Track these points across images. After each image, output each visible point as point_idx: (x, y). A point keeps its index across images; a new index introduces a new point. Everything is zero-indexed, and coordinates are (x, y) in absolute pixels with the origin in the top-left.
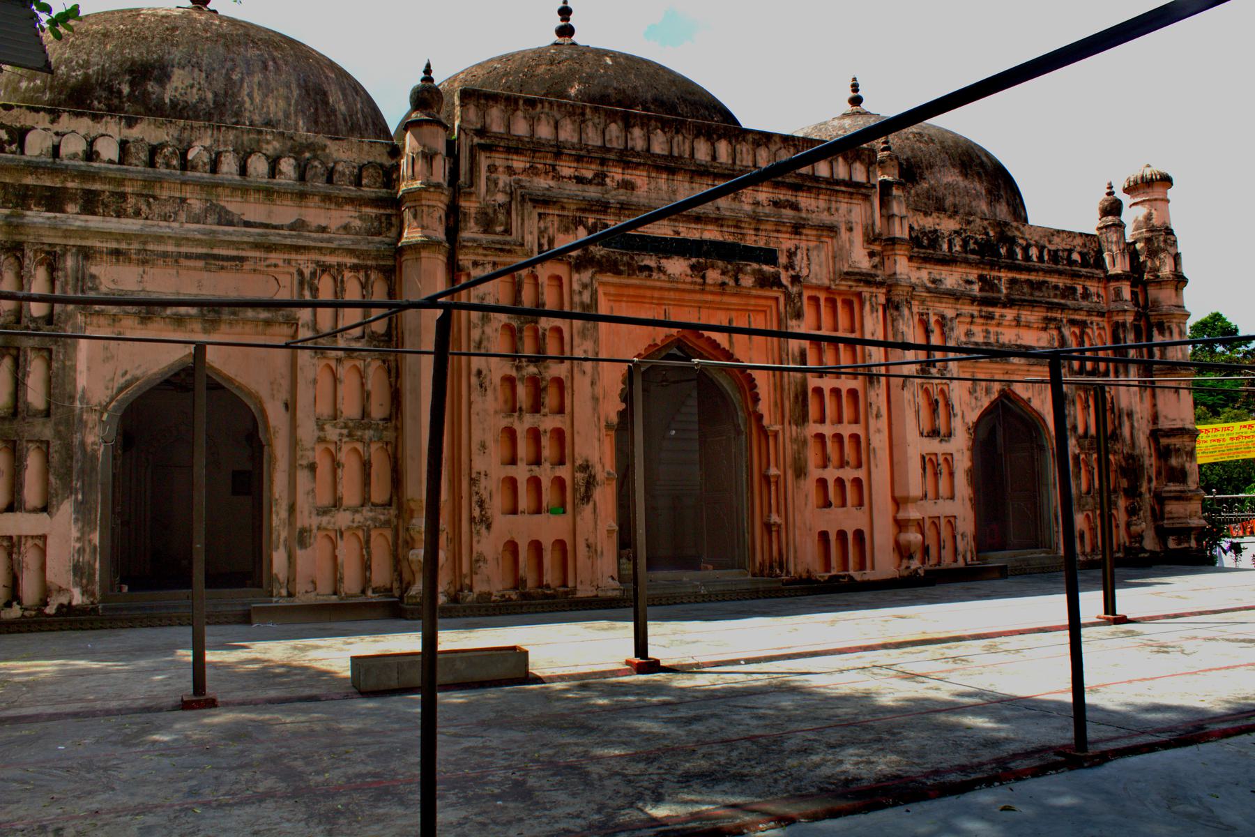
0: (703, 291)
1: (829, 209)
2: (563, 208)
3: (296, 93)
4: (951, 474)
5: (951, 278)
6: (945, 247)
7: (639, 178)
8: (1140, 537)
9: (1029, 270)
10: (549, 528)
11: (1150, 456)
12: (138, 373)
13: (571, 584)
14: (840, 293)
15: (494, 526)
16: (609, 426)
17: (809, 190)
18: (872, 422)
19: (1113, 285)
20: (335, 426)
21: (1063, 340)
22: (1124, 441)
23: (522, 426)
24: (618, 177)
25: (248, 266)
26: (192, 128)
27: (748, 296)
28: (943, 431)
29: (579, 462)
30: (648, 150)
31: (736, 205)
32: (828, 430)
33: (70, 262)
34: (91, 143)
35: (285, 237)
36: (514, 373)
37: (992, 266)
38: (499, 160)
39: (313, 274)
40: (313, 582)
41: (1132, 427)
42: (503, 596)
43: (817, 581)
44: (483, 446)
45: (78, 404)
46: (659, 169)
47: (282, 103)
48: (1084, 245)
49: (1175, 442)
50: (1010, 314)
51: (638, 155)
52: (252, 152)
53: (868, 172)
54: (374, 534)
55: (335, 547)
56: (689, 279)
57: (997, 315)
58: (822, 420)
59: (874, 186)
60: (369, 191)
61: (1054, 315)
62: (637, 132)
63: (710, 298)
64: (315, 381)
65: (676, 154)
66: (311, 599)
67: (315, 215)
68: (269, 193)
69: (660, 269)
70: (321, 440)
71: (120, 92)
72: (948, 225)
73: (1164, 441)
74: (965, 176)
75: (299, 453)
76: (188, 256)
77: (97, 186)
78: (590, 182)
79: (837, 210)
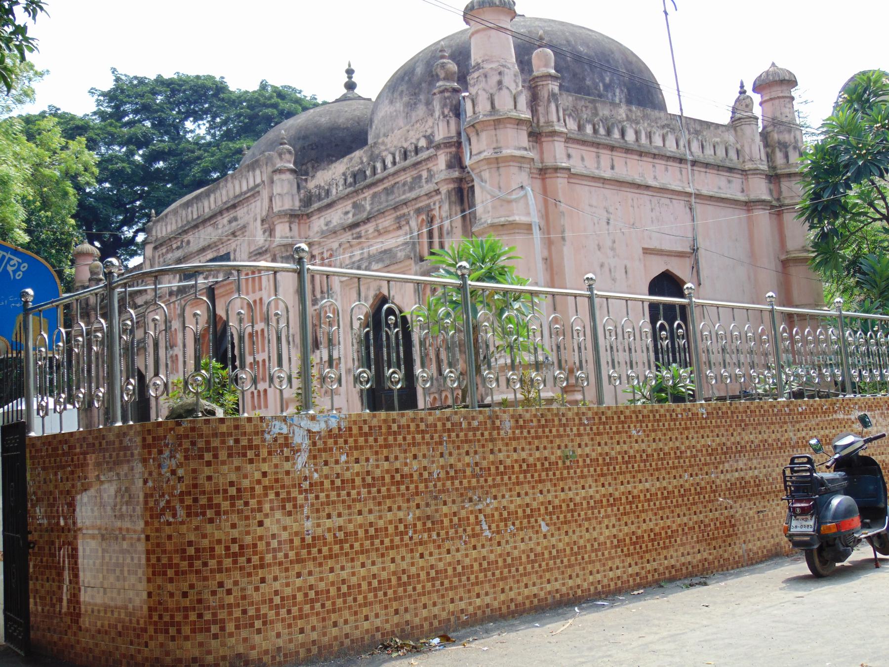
5: (336, 216)
7: (190, 237)
50: (370, 227)
61: (402, 212)
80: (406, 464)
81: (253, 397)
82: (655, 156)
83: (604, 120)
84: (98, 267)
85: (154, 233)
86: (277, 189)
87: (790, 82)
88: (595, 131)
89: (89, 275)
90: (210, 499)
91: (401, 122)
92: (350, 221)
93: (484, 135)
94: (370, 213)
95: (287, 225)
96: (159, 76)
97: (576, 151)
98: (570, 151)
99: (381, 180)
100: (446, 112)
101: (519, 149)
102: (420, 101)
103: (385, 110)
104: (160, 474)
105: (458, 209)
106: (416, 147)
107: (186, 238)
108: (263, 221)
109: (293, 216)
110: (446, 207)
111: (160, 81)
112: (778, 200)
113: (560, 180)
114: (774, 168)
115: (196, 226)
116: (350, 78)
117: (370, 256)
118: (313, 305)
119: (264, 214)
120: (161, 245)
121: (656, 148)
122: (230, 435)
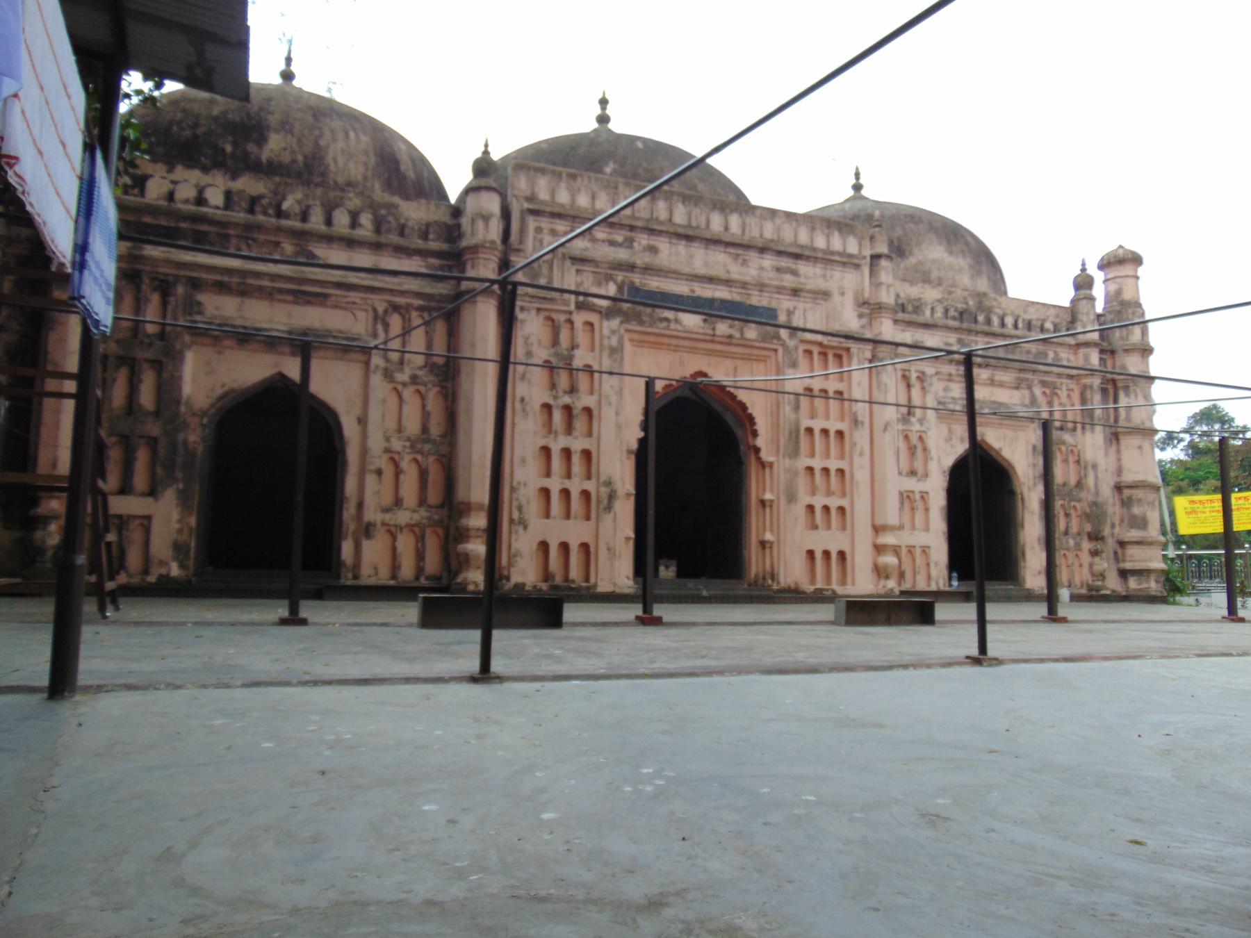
0: (712, 341)
1: (824, 276)
2: (597, 266)
3: (373, 160)
4: (927, 510)
5: (932, 339)
6: (928, 313)
7: (663, 244)
8: (1102, 576)
9: (1004, 336)
10: (575, 532)
11: (1114, 505)
12: (235, 385)
13: (592, 580)
14: (832, 348)
15: (531, 528)
16: (629, 452)
17: (808, 258)
18: (856, 459)
19: (1082, 351)
20: (399, 439)
21: (1034, 401)
22: (1089, 491)
23: (556, 447)
24: (644, 242)
25: (330, 302)
26: (286, 184)
27: (752, 347)
28: (920, 471)
29: (603, 478)
30: (670, 220)
31: (742, 269)
32: (817, 464)
33: (180, 290)
34: (201, 191)
35: (362, 279)
36: (551, 402)
37: (970, 331)
38: (545, 223)
39: (386, 312)
40: (376, 569)
41: (1096, 478)
42: (535, 587)
43: (804, 593)
44: (523, 461)
45: (183, 409)
46: (678, 236)
47: (361, 169)
48: (1058, 316)
49: (1138, 493)
51: (662, 223)
52: (337, 206)
53: (860, 245)
54: (428, 531)
55: (394, 539)
56: (701, 331)
58: (812, 455)
59: (864, 257)
60: (434, 245)
62: (661, 205)
63: (719, 347)
64: (384, 401)
65: (694, 223)
66: (373, 581)
67: (389, 262)
68: (350, 243)
69: (677, 321)
70: (387, 450)
71: (223, 150)
72: (931, 294)
73: (1127, 492)
74: (951, 253)
75: (368, 459)
76: (281, 291)
77: (205, 228)
78: (620, 245)
79: (831, 277)
107: (643, 240)
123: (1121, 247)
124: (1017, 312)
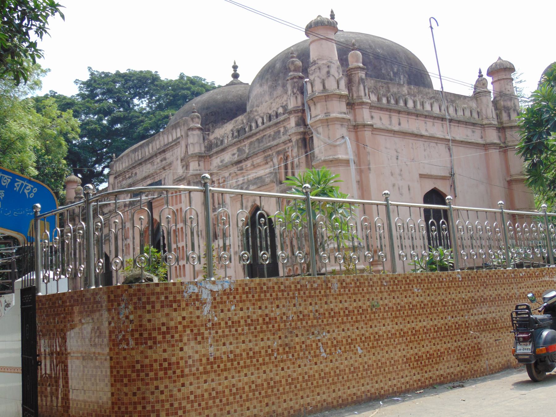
5: (227, 157)
7: (137, 170)
24: (134, 172)
50: (249, 163)
57: (244, 167)
59: (182, 136)
61: (268, 153)
80: (272, 311)
81: (176, 270)
82: (426, 117)
83: (394, 95)
84: (80, 190)
85: (115, 169)
86: (191, 140)
87: (511, 69)
88: (388, 101)
89: (75, 195)
90: (150, 334)
91: (267, 98)
92: (236, 159)
93: (319, 106)
94: (248, 154)
95: (197, 163)
96: (118, 72)
97: (377, 114)
98: (373, 114)
99: (255, 134)
100: (295, 91)
101: (341, 113)
102: (279, 84)
103: (257, 90)
104: (119, 318)
105: (303, 151)
106: (277, 113)
108: (182, 160)
109: (201, 157)
110: (295, 150)
111: (118, 74)
112: (504, 143)
113: (366, 133)
114: (502, 123)
115: (140, 164)
116: (235, 71)
117: (248, 181)
118: (213, 212)
119: (183, 155)
120: (119, 175)
121: (427, 111)
122: (162, 293)
123: (319, 16)
124: (266, 112)
